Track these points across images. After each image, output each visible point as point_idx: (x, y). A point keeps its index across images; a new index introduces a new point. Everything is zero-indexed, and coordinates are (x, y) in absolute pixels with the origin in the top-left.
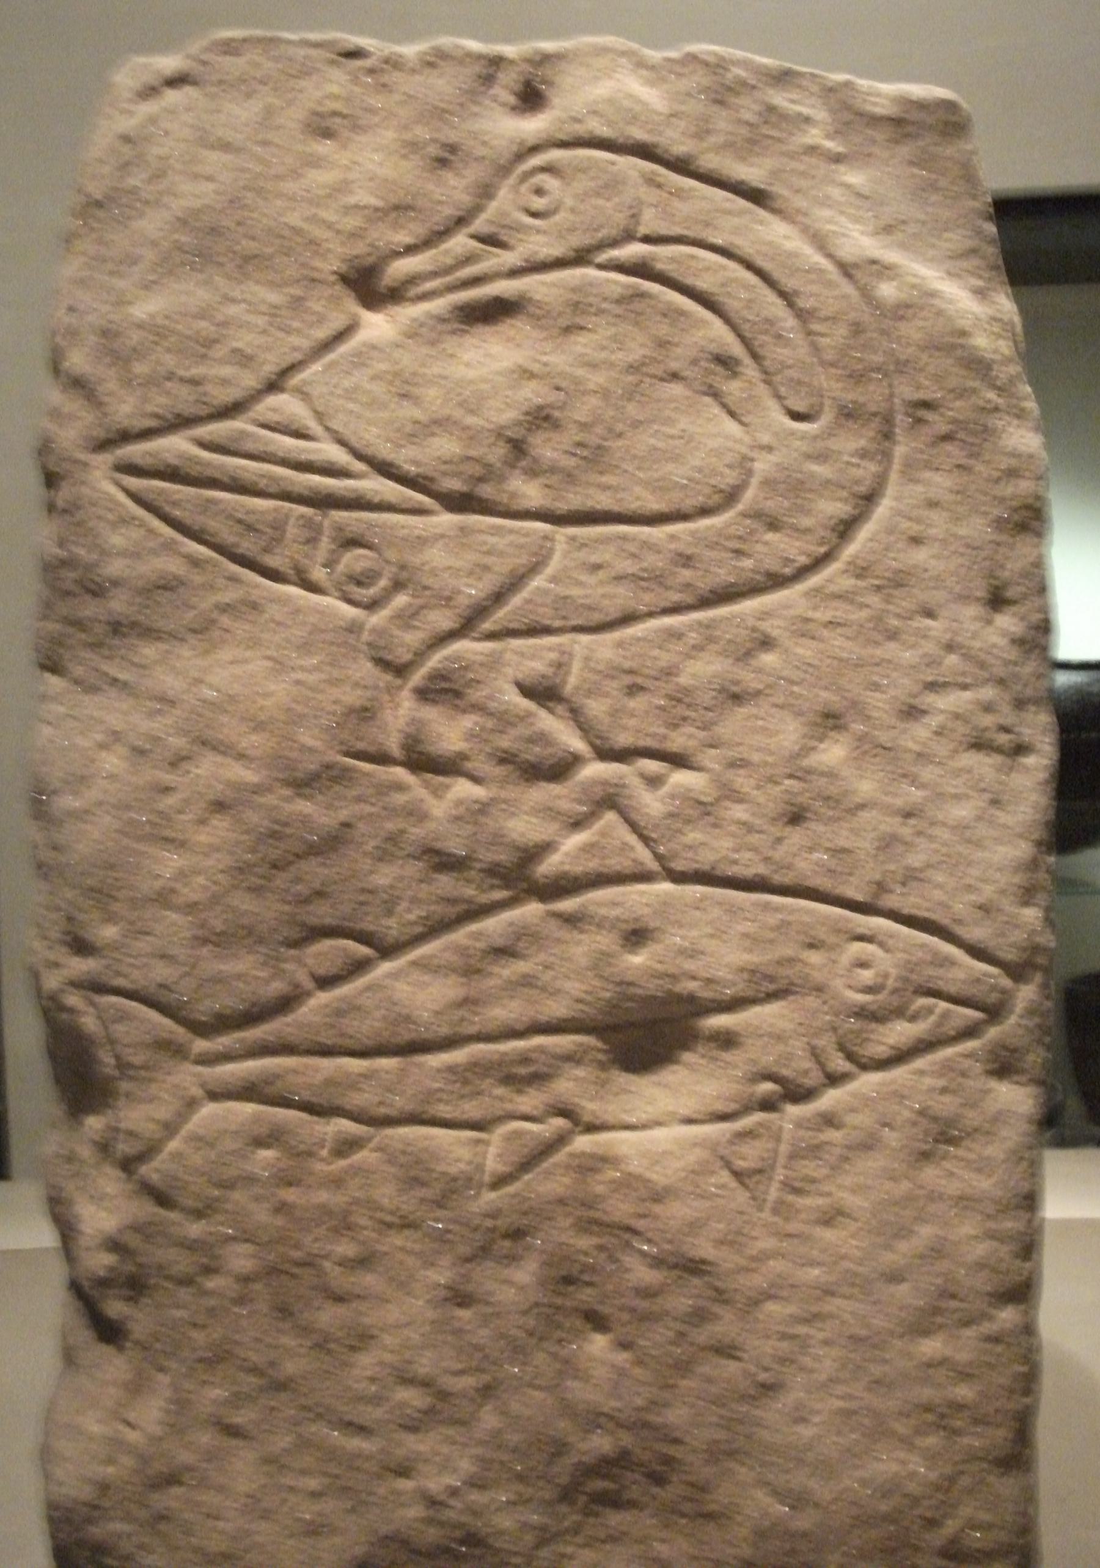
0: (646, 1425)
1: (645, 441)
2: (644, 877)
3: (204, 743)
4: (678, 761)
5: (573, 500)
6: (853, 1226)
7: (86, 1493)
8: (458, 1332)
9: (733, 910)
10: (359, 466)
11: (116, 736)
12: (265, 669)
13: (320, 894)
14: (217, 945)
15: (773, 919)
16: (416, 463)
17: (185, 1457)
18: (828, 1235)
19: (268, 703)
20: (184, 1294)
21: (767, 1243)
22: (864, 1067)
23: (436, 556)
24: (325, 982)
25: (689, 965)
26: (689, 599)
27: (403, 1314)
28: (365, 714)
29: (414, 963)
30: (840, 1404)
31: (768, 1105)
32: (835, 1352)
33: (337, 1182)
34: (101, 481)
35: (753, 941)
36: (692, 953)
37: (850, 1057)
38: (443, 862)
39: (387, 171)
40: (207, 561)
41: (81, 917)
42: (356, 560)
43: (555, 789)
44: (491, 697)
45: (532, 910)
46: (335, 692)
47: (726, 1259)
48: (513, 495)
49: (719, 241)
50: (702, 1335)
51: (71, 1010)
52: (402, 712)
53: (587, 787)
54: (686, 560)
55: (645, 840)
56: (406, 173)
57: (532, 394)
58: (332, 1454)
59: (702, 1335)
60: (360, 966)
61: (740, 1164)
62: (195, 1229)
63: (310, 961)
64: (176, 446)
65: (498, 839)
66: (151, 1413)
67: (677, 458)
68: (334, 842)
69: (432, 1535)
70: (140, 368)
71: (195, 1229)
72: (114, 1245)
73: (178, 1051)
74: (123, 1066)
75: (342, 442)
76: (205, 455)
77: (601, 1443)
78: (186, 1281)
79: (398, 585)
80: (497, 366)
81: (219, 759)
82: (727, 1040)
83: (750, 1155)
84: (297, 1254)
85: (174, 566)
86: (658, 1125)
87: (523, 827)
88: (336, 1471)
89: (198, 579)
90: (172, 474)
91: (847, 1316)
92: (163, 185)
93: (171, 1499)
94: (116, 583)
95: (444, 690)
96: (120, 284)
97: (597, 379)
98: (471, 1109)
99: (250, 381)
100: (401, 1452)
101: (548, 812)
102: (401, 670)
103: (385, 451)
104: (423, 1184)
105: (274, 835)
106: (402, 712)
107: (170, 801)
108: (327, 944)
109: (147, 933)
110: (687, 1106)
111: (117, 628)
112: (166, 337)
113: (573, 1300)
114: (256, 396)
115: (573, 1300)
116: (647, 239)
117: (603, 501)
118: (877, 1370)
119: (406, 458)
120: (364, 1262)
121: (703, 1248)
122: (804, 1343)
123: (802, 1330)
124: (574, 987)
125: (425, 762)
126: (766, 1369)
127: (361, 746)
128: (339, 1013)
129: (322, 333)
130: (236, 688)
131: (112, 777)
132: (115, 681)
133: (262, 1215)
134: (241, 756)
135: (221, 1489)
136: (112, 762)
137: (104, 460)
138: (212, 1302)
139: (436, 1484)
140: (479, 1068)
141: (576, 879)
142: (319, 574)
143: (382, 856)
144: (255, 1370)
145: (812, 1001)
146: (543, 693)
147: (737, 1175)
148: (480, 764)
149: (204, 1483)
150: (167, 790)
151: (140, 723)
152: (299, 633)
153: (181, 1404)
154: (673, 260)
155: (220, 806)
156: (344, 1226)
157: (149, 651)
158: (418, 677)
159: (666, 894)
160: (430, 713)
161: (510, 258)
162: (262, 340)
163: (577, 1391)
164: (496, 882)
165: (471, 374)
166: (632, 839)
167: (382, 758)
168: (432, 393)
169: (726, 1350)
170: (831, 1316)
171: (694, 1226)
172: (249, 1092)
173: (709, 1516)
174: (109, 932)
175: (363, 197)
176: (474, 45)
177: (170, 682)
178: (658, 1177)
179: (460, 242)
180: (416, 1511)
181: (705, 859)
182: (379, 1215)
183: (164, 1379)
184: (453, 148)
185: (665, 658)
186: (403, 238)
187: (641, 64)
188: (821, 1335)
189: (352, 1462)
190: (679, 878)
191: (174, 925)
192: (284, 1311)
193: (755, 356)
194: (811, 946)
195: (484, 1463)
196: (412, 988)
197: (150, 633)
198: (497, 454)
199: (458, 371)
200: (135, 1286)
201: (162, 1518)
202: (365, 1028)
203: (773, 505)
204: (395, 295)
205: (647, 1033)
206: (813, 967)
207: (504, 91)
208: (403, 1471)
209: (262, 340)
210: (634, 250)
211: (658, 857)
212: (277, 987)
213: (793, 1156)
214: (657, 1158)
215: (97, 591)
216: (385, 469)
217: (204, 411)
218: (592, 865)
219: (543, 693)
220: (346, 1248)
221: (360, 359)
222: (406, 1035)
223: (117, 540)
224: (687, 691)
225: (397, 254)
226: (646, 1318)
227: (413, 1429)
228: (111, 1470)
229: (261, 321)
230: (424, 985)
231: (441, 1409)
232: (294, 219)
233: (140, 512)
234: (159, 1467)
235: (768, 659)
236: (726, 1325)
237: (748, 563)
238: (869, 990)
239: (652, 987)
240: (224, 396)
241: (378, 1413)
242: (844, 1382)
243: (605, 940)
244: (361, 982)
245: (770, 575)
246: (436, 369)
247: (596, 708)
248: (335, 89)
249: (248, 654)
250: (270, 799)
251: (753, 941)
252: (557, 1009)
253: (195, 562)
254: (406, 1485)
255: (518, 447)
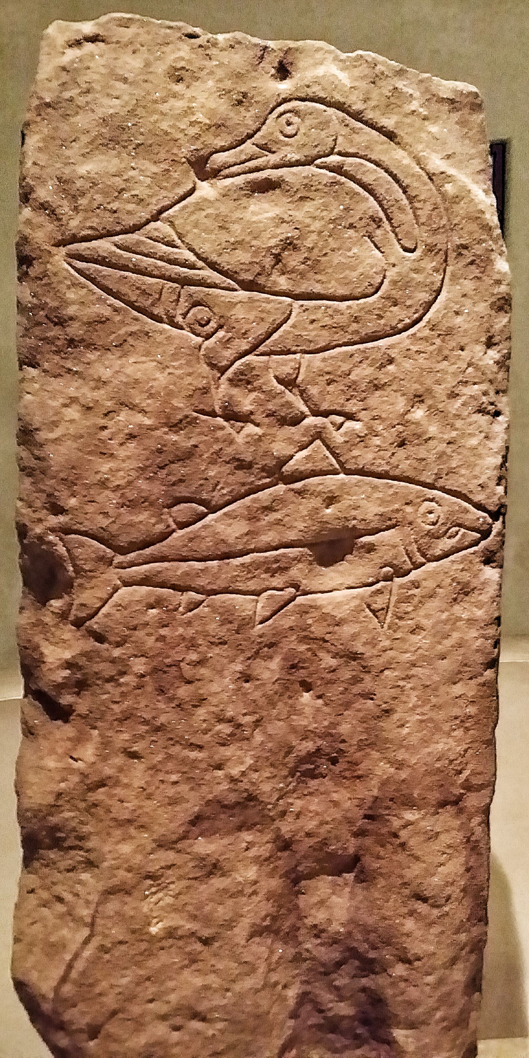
0: (331, 735)
1: (337, 258)
2: (336, 473)
3: (121, 404)
4: (350, 417)
5: (304, 288)
6: (424, 633)
7: (50, 800)
8: (245, 694)
9: (375, 488)
10: (200, 264)
11: (74, 400)
12: (154, 367)
13: (181, 481)
14: (128, 507)
15: (391, 491)
16: (228, 264)
17: (108, 771)
18: (415, 638)
19: (155, 384)
20: (109, 686)
21: (387, 643)
22: (429, 561)
23: (239, 313)
24: (182, 525)
25: (354, 513)
26: (356, 338)
27: (220, 686)
28: (205, 391)
29: (225, 514)
30: (418, 717)
31: (388, 578)
32: (415, 693)
33: (189, 623)
34: (59, 260)
35: (383, 502)
36: (356, 508)
37: (424, 555)
38: (242, 465)
39: (212, 104)
40: (121, 308)
41: (56, 493)
42: (199, 312)
43: (293, 429)
44: (264, 384)
45: (281, 488)
46: (189, 379)
47: (368, 651)
48: (275, 282)
49: (373, 157)
50: (356, 689)
51: (50, 543)
52: (222, 391)
53: (308, 428)
54: (356, 320)
55: (333, 453)
56: (222, 107)
57: (287, 231)
58: (184, 761)
59: (356, 689)
60: (202, 516)
61: (374, 606)
62: (117, 652)
63: (173, 515)
64: (104, 246)
65: (267, 453)
66: (88, 752)
67: (353, 269)
68: (188, 455)
69: (232, 798)
70: (83, 202)
71: (117, 652)
72: (69, 665)
73: (110, 562)
74: (78, 570)
75: (192, 250)
76: (118, 251)
77: (309, 746)
78: (110, 680)
79: (221, 327)
80: (267, 215)
81: (130, 412)
82: (370, 548)
83: (379, 602)
84: (167, 661)
85: (107, 312)
86: (338, 590)
87: (279, 448)
88: (185, 770)
89: (118, 318)
90: (102, 261)
91: (421, 676)
92: (89, 97)
93: (100, 794)
94: (71, 319)
95: (244, 380)
96: (68, 153)
97: (316, 225)
98: (252, 585)
99: (145, 215)
100: (216, 757)
101: (290, 440)
102: (223, 371)
103: (214, 257)
104: (231, 622)
105: (160, 451)
106: (222, 391)
107: (106, 433)
108: (183, 506)
109: (93, 502)
110: (350, 581)
111: (71, 342)
112: (96, 185)
113: (299, 676)
114: (148, 222)
115: (299, 676)
116: (340, 154)
117: (318, 288)
118: (434, 700)
119: (226, 261)
120: (201, 663)
121: (359, 648)
122: (402, 688)
123: (401, 683)
124: (301, 525)
125: (233, 415)
126: (386, 703)
127: (201, 407)
128: (191, 540)
129: (181, 191)
130: (139, 375)
131: (72, 421)
132: (69, 371)
133: (150, 642)
134: (143, 411)
135: (127, 786)
136: (73, 413)
137: (63, 251)
138: (123, 689)
139: (235, 771)
140: (256, 565)
141: (301, 472)
142: (179, 319)
143: (213, 462)
144: (146, 722)
145: (407, 529)
146: (289, 383)
147: (374, 612)
148: (258, 417)
149: (117, 783)
150: (104, 428)
151: (88, 394)
152: (171, 350)
153: (106, 743)
154: (351, 165)
155: (131, 436)
156: (192, 645)
157: (92, 356)
158: (229, 373)
159: (343, 479)
160: (235, 391)
161: (273, 159)
162: (148, 191)
163: (299, 722)
164: (264, 474)
165: (255, 218)
166: (328, 453)
167: (213, 414)
168: (236, 228)
169: (369, 696)
170: (413, 676)
171: (354, 637)
172: (145, 581)
173: (359, 777)
174: (73, 502)
175: (200, 117)
176: (256, 40)
177: (106, 374)
178: (339, 614)
179: (248, 147)
180: (225, 786)
181: (361, 463)
182: (209, 638)
183: (96, 732)
184: (245, 95)
185: (345, 367)
186: (219, 143)
187: (336, 59)
188: (409, 686)
189: (194, 764)
190: (349, 472)
191: (109, 499)
192: (161, 691)
193: (389, 219)
194: (407, 504)
195: (257, 759)
196: (224, 526)
197: (90, 346)
198: (268, 261)
199: (247, 215)
200: (81, 686)
201: (95, 805)
202: (206, 546)
203: (396, 294)
204: (215, 174)
205: (332, 547)
206: (408, 513)
207: (269, 66)
208: (219, 767)
209: (148, 191)
210: (334, 159)
211: (339, 462)
212: (160, 527)
213: (399, 601)
214: (339, 605)
215: (61, 322)
216: (213, 266)
217: (118, 229)
218: (309, 466)
219: (289, 383)
220: (194, 656)
221: (199, 207)
222: (225, 549)
223: (71, 295)
224: (354, 382)
225: (217, 152)
226: (331, 682)
227: (223, 745)
228: (63, 785)
229: (148, 180)
230: (230, 525)
231: (238, 734)
232: (164, 126)
233: (83, 280)
234: (94, 778)
235: (391, 368)
236: (368, 683)
237: (382, 322)
238: (434, 524)
239: (337, 525)
240: (131, 221)
241: (207, 737)
242: (419, 706)
243: (316, 502)
244: (199, 525)
245: (392, 328)
246: (238, 214)
247: (313, 391)
248: (182, 54)
249: (144, 359)
250: (158, 433)
251: (383, 502)
252: (292, 536)
253: (116, 310)
254: (220, 773)
255: (278, 258)
